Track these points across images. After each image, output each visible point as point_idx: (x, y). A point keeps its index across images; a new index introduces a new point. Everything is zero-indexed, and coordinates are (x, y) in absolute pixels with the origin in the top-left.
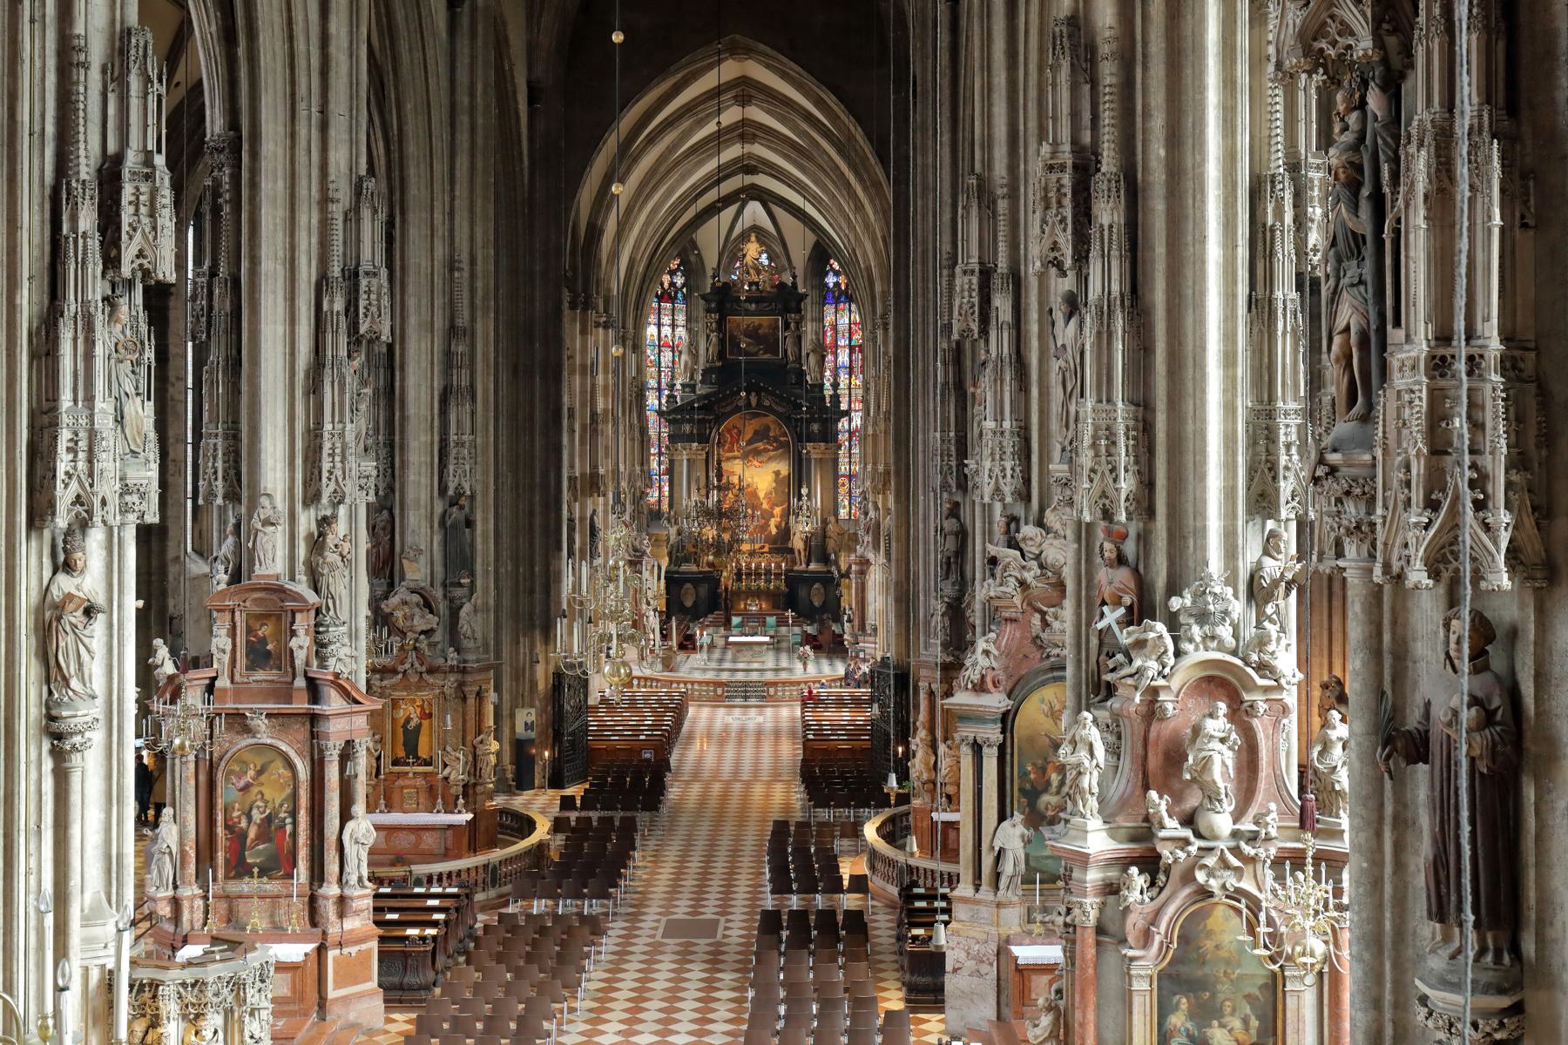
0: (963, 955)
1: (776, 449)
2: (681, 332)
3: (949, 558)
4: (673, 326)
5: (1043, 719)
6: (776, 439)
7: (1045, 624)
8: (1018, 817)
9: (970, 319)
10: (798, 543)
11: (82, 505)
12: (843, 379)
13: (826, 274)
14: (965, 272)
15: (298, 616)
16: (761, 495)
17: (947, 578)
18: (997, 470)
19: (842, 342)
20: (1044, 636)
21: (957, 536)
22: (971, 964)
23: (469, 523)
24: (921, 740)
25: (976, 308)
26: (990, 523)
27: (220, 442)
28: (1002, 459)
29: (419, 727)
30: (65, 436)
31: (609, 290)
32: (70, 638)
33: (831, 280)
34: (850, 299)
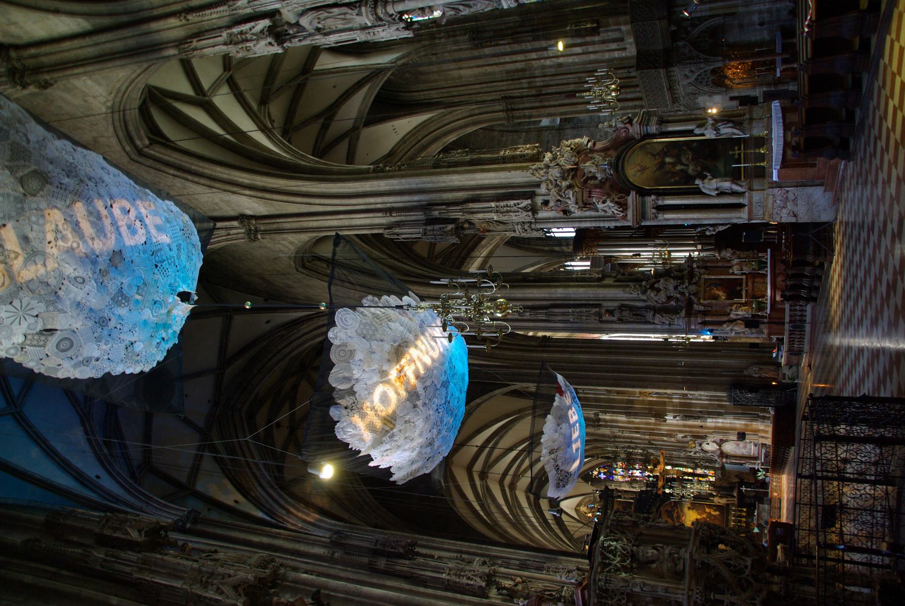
0: (784, 211)
1: (677, 508)
3: (634, 315)
6: (673, 507)
8: (697, 182)
9: (446, 229)
10: (723, 501)
11: (239, 585)
13: (600, 478)
17: (645, 316)
18: (515, 208)
20: (599, 176)
21: (622, 310)
22: (790, 205)
24: (728, 326)
25: (441, 226)
26: (550, 219)
28: (510, 206)
33: (602, 476)
34: (611, 466)
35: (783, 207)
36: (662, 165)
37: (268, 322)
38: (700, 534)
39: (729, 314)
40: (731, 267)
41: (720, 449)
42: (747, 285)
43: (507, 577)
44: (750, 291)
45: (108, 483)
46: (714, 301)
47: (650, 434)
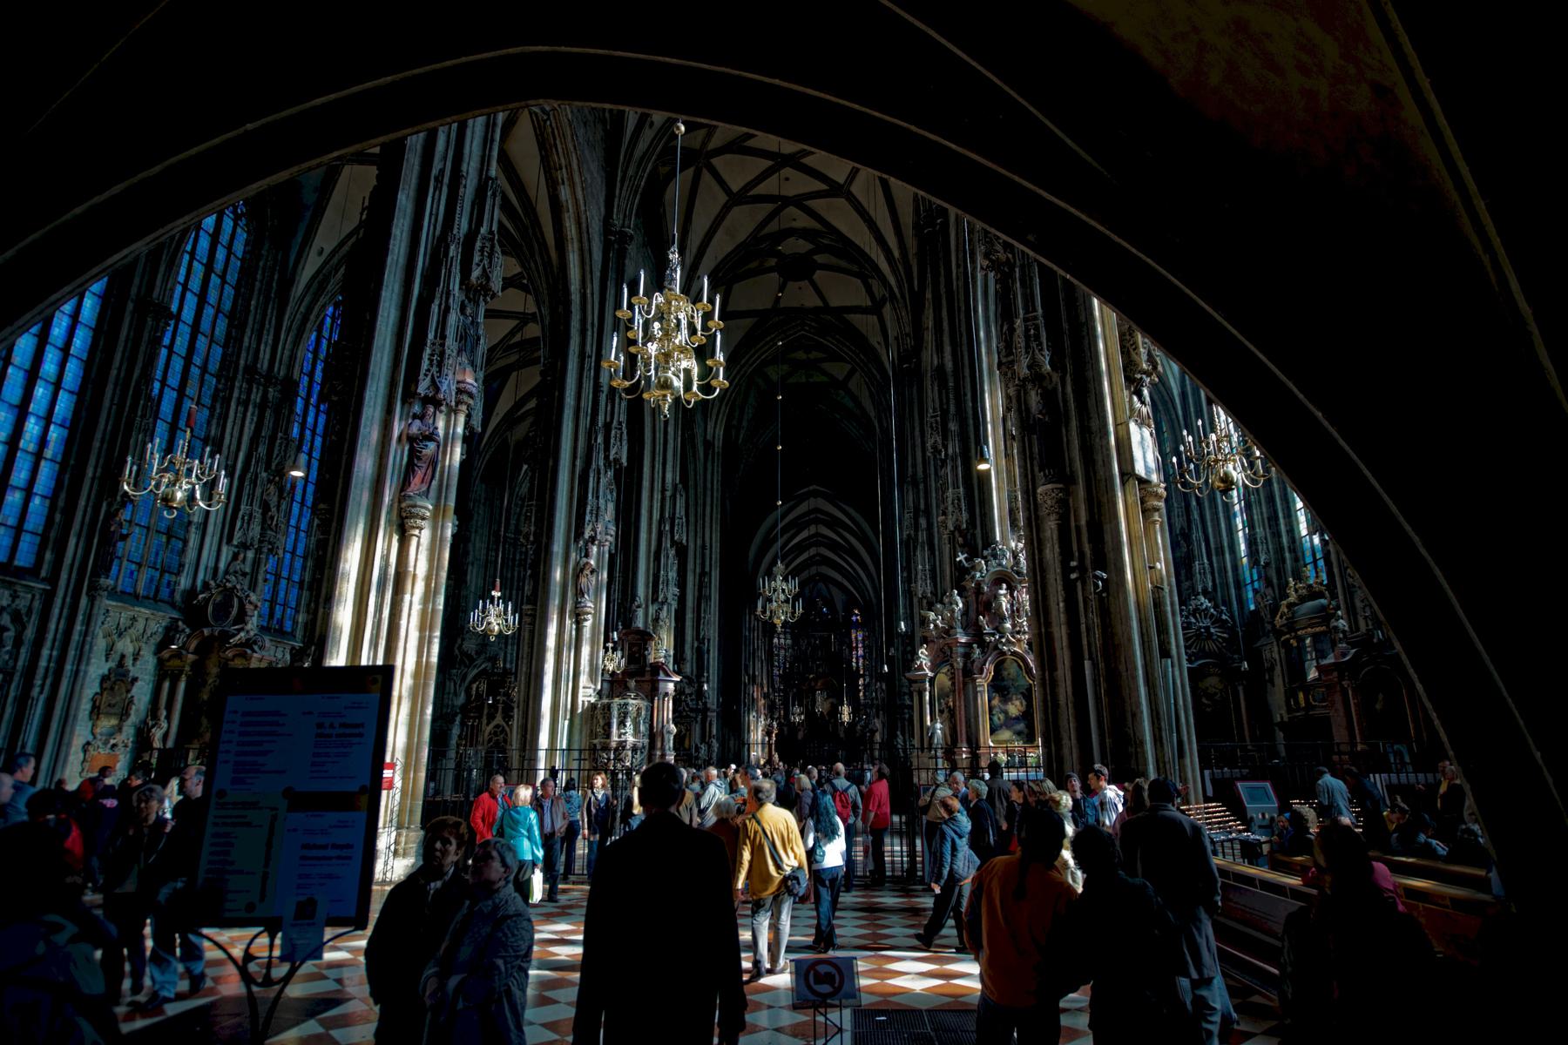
2: (789, 642)
4: (785, 639)
19: (860, 645)
29: (685, 734)
30: (589, 508)
33: (854, 618)
37: (879, 343)
43: (669, 611)
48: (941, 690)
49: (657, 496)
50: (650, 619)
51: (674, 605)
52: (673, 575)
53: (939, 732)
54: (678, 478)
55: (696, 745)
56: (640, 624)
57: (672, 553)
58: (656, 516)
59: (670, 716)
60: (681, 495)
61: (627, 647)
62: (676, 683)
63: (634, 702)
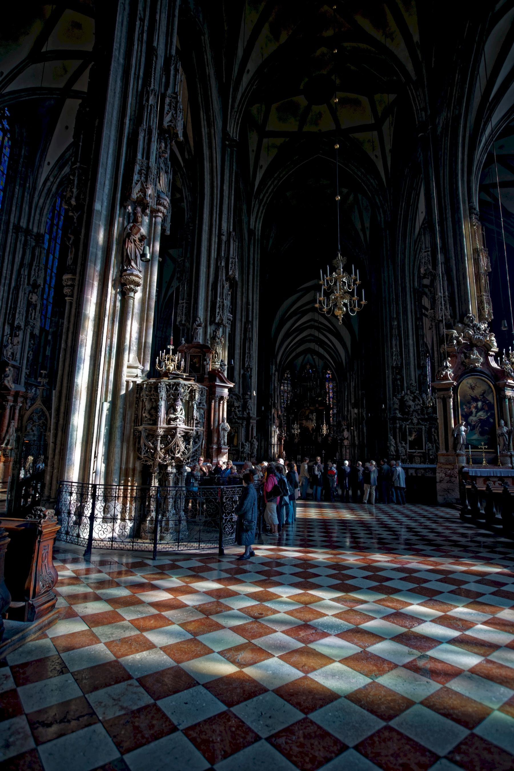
0: (444, 475)
2: (289, 388)
4: (287, 387)
5: (468, 389)
7: (466, 357)
9: (429, 265)
12: (331, 400)
14: (425, 252)
15: (207, 354)
16: (310, 429)
19: (331, 391)
20: (467, 361)
22: (447, 478)
23: (251, 377)
26: (439, 331)
27: (184, 304)
30: (137, 168)
31: (276, 362)
32: (133, 245)
33: (327, 376)
35: (446, 475)
36: (476, 400)
37: (376, 156)
38: (191, 431)
39: (400, 442)
40: (431, 443)
41: (345, 439)
42: (419, 453)
43: (224, 332)
44: (415, 454)
45: (246, 79)
46: (408, 433)
47: (348, 401)
48: (464, 396)
49: (215, 240)
50: (208, 337)
51: (228, 330)
52: (227, 303)
53: (464, 433)
54: (232, 227)
55: (242, 444)
56: (200, 340)
57: (227, 286)
58: (214, 255)
59: (225, 416)
60: (234, 241)
61: (189, 359)
62: (230, 390)
63: (186, 383)
